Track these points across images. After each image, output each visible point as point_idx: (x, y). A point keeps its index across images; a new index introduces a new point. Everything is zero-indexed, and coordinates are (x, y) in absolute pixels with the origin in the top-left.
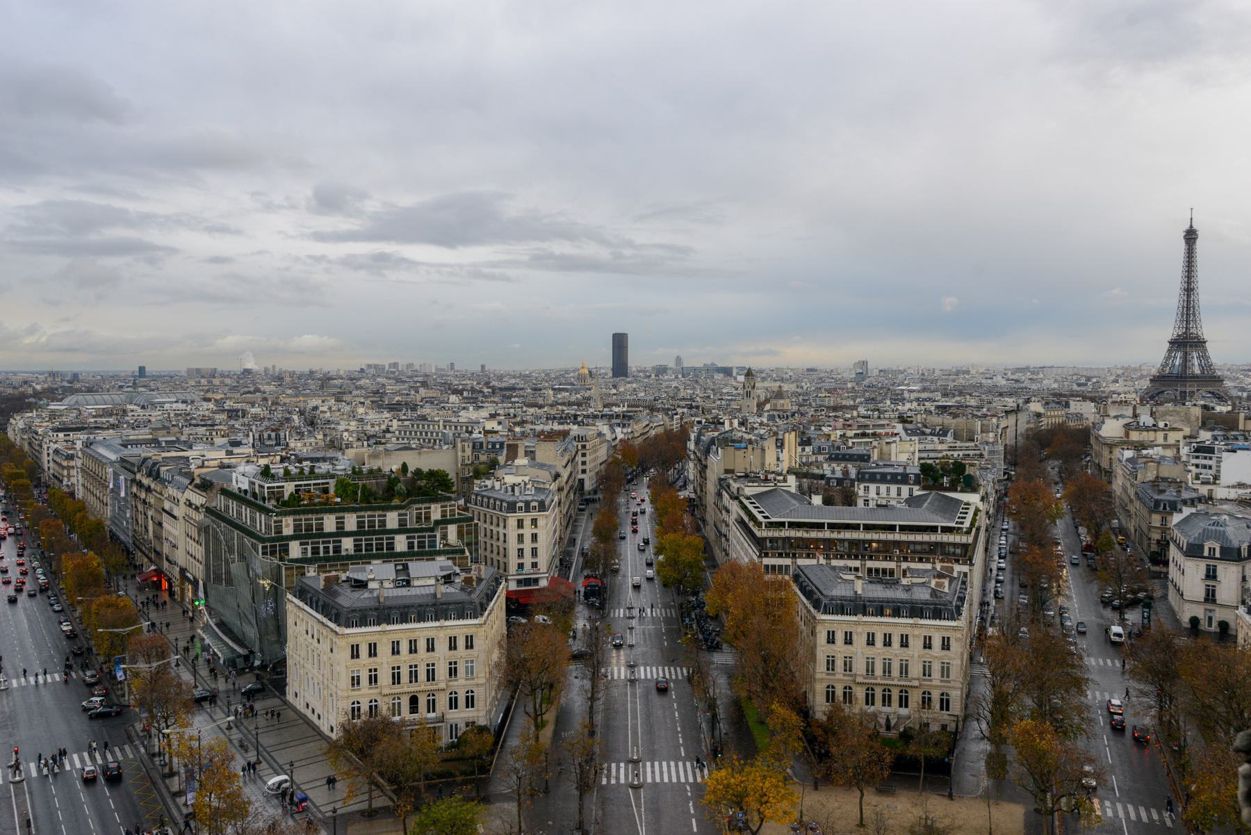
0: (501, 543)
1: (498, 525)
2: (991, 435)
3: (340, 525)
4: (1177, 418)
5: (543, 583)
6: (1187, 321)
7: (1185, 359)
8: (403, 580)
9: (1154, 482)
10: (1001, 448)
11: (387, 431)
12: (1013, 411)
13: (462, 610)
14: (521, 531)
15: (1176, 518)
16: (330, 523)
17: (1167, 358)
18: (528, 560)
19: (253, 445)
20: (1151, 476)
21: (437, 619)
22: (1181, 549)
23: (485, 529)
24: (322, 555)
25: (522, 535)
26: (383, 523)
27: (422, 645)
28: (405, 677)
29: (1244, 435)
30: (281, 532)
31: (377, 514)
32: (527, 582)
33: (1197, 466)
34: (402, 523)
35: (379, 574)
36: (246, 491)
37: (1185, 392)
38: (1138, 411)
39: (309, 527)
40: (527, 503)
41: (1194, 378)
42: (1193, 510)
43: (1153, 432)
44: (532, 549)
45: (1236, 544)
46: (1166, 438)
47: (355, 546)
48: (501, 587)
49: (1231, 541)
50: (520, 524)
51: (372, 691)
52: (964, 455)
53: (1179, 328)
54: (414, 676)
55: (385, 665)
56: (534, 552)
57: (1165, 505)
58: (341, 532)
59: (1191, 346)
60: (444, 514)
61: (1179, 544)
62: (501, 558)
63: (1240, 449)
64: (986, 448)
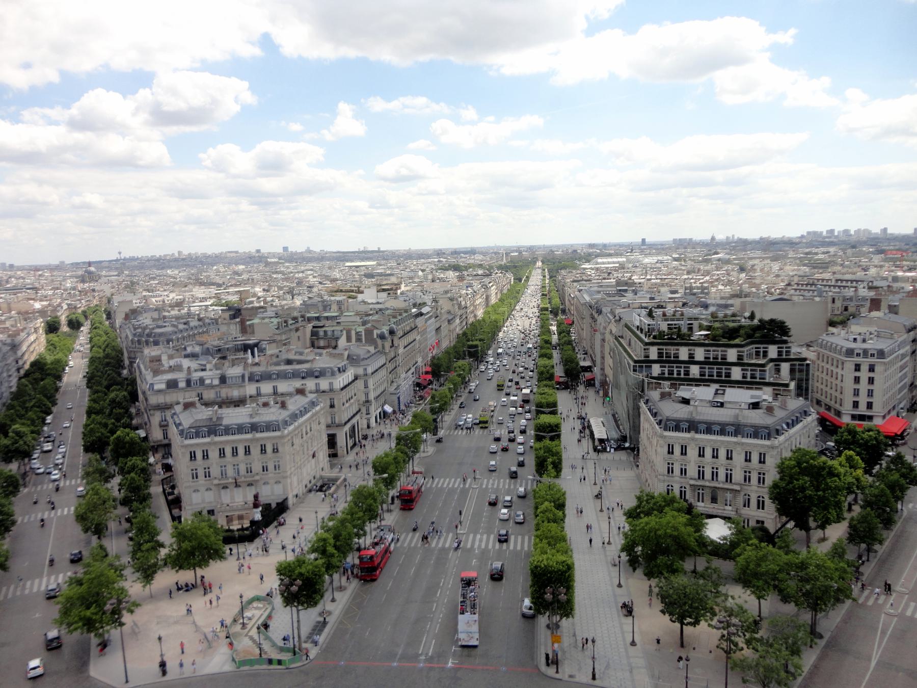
0: (838, 382)
1: (837, 367)
3: (691, 356)
5: (878, 421)
8: (717, 402)
11: (789, 285)
13: (757, 432)
14: (857, 374)
16: (684, 353)
18: (863, 400)
19: (685, 293)
21: (736, 436)
23: (823, 367)
24: (675, 376)
25: (859, 377)
26: (724, 357)
27: (722, 454)
28: (708, 475)
30: (648, 357)
31: (720, 349)
32: (862, 418)
34: (740, 357)
35: (705, 393)
36: (638, 327)
39: (668, 356)
40: (865, 352)
44: (869, 390)
47: (700, 372)
48: (809, 419)
50: (858, 368)
51: (682, 480)
54: (715, 475)
55: (692, 463)
56: (870, 393)
58: (692, 361)
60: (780, 353)
62: (838, 394)
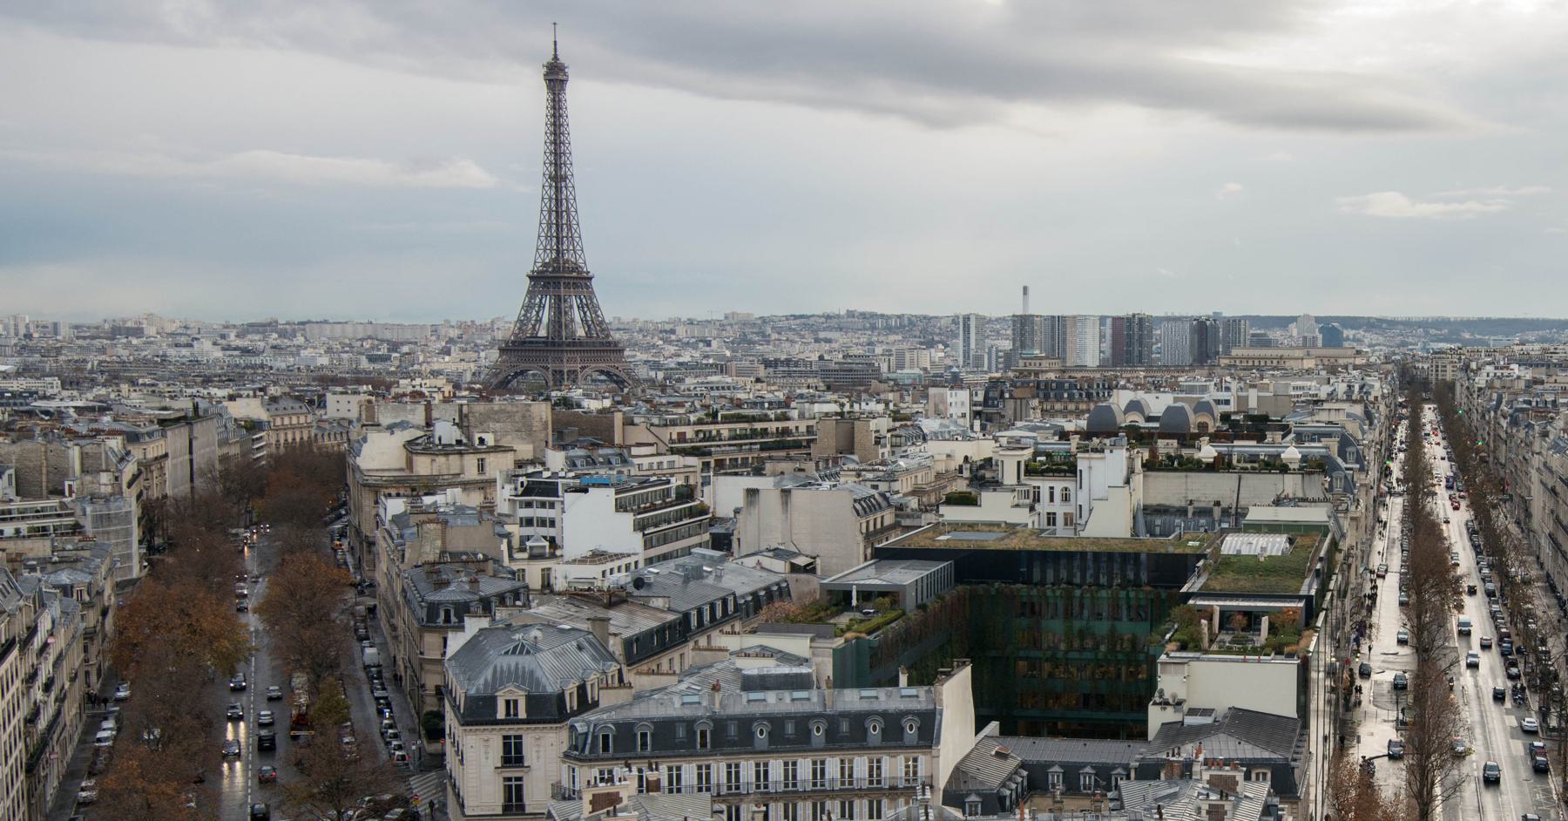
2: (105, 478)
4: (509, 426)
6: (557, 238)
7: (559, 311)
9: (434, 564)
10: (134, 509)
12: (185, 418)
15: (456, 642)
17: (528, 308)
20: (430, 552)
22: (456, 708)
29: (621, 455)
33: (529, 522)
37: (561, 372)
38: (435, 414)
41: (576, 344)
42: (484, 623)
43: (457, 457)
45: (551, 688)
46: (481, 467)
49: (544, 687)
52: (31, 529)
53: (545, 250)
57: (447, 613)
59: (567, 286)
61: (455, 701)
63: (594, 485)
64: (89, 509)
